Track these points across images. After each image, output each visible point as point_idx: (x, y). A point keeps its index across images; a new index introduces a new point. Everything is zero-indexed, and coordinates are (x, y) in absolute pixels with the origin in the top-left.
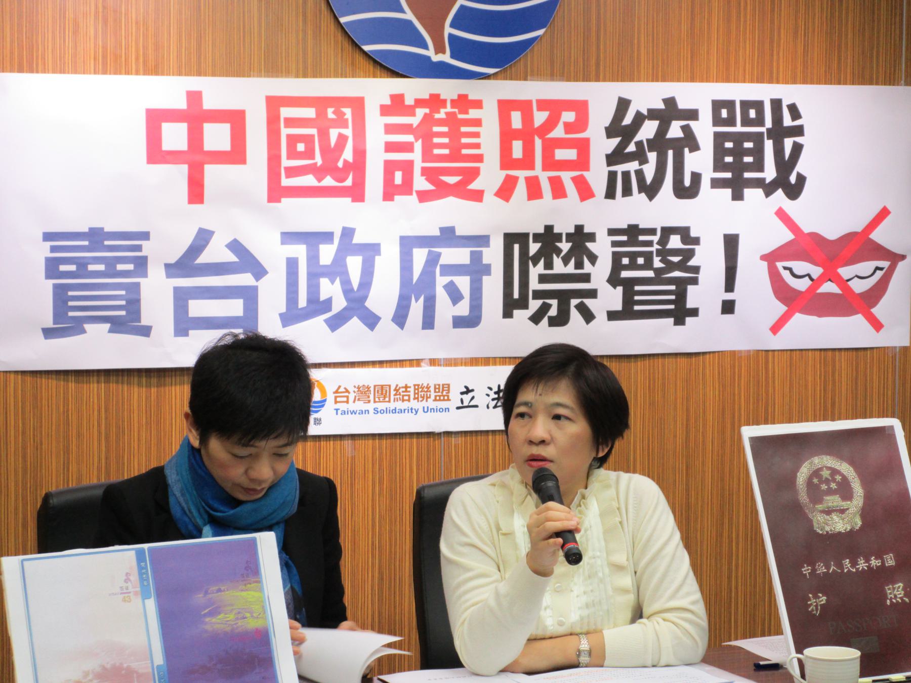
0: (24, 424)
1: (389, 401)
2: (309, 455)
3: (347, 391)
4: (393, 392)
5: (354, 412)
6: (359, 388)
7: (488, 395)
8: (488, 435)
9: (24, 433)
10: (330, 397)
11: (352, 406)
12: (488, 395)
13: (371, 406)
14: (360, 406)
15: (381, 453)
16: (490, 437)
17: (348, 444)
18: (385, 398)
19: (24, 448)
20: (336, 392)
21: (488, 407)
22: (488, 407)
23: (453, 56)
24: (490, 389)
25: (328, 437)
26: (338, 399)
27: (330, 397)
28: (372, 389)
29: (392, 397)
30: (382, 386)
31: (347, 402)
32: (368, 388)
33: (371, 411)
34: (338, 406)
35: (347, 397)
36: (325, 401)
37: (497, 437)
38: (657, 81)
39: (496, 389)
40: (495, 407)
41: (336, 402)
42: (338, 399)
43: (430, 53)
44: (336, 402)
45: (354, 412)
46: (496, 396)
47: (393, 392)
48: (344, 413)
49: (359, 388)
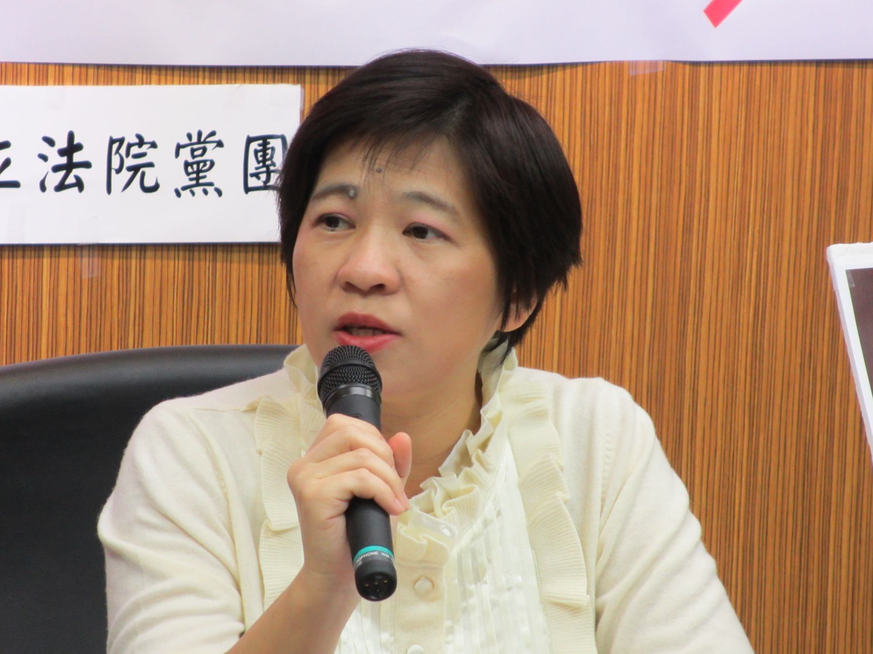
7: (44, 158)
8: (40, 257)
12: (44, 158)
16: (46, 261)
21: (43, 188)
22: (43, 188)
24: (50, 142)
37: (63, 261)
39: (62, 143)
40: (61, 187)
46: (64, 160)
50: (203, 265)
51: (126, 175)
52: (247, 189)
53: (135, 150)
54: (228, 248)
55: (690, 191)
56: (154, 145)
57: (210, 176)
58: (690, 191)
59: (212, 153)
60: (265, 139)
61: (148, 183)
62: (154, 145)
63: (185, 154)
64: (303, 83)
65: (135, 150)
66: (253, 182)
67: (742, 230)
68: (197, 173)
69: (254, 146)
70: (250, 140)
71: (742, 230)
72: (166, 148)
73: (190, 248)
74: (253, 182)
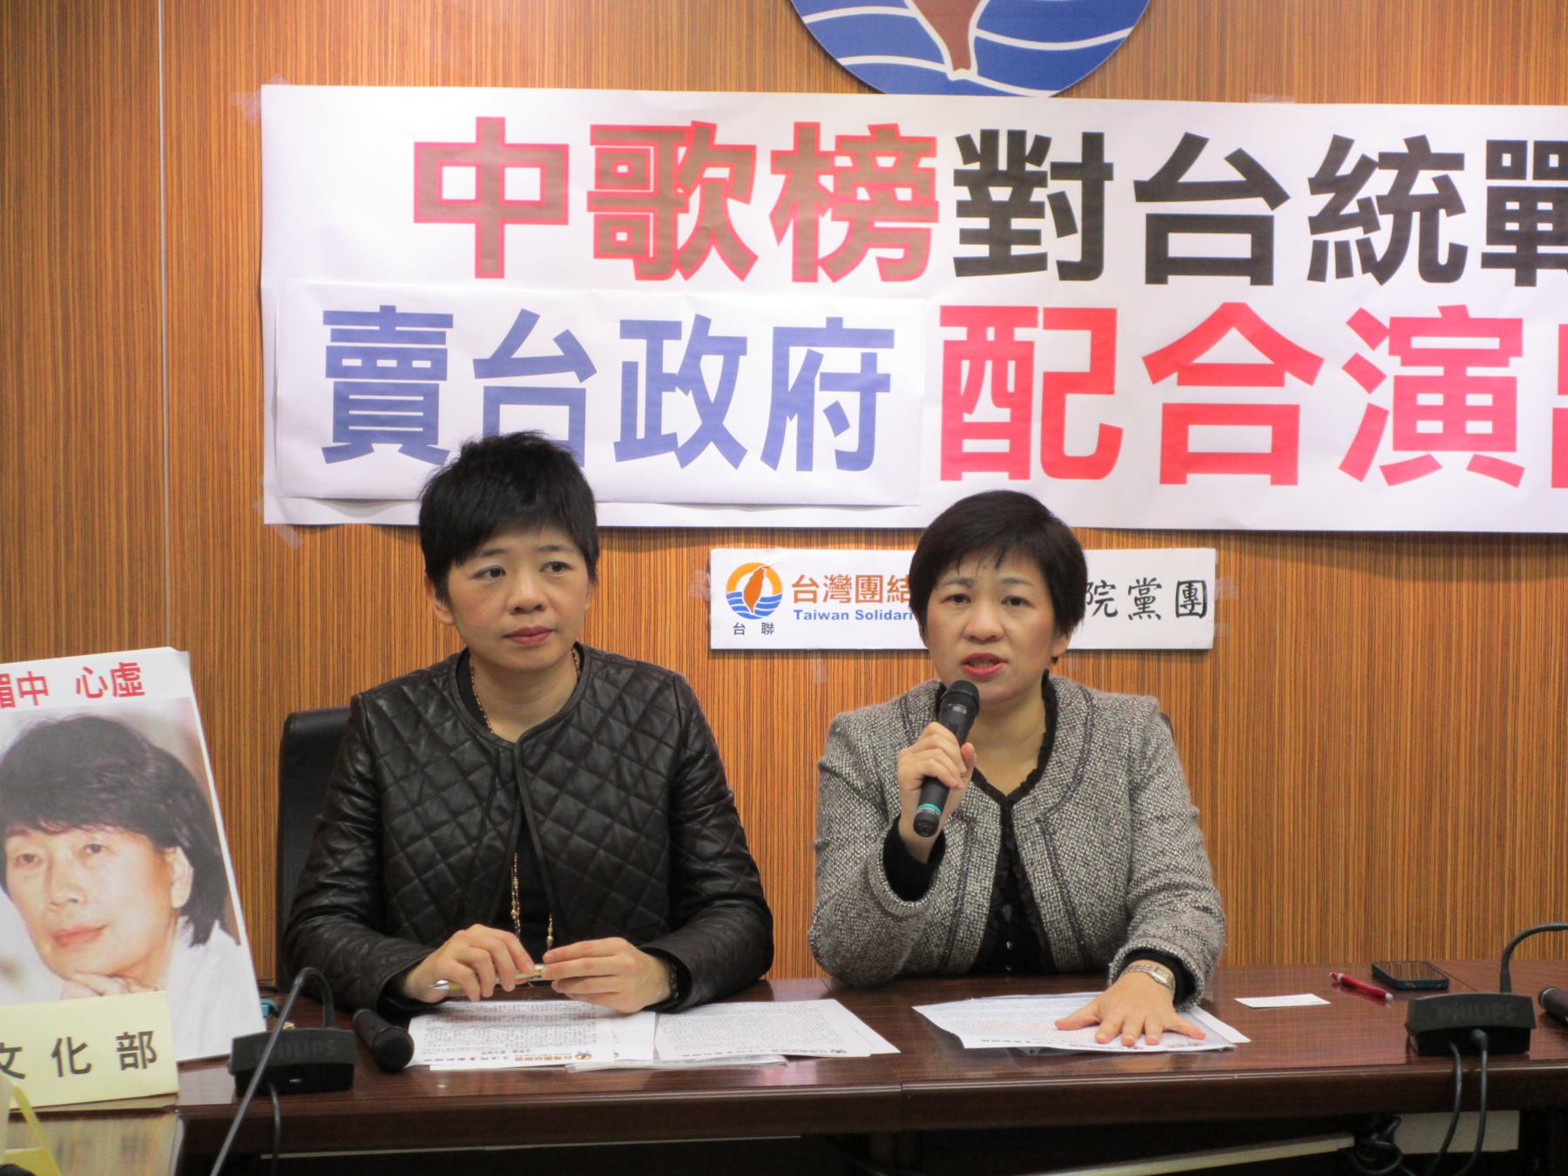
0: (323, 620)
1: (880, 601)
2: (755, 678)
3: (814, 584)
4: (886, 588)
5: (824, 616)
6: (832, 579)
9: (324, 634)
10: (788, 592)
11: (821, 607)
13: (851, 608)
14: (834, 606)
15: (868, 680)
17: (816, 664)
18: (873, 595)
19: (325, 657)
20: (797, 584)
23: (981, 73)
25: (785, 653)
26: (800, 596)
27: (788, 592)
28: (853, 581)
29: (885, 595)
30: (869, 577)
31: (814, 600)
32: (847, 579)
33: (852, 615)
34: (800, 605)
35: (815, 593)
36: (779, 597)
38: (1321, 101)
41: (797, 600)
42: (800, 596)
43: (947, 68)
44: (797, 600)
45: (824, 616)
47: (886, 588)
48: (809, 616)
49: (832, 579)
50: (1152, 663)
51: (1094, 606)
52: (1178, 615)
53: (1100, 590)
54: (1169, 652)
55: (1507, 618)
56: (1113, 587)
57: (1152, 607)
58: (1507, 618)
59: (1153, 592)
60: (1190, 583)
61: (1110, 611)
62: (1113, 587)
63: (1135, 593)
64: (1217, 547)
65: (1100, 590)
66: (1182, 610)
67: (1548, 644)
68: (1144, 605)
69: (1183, 587)
70: (1180, 584)
71: (1548, 644)
72: (1122, 589)
73: (1142, 653)
74: (1182, 610)
